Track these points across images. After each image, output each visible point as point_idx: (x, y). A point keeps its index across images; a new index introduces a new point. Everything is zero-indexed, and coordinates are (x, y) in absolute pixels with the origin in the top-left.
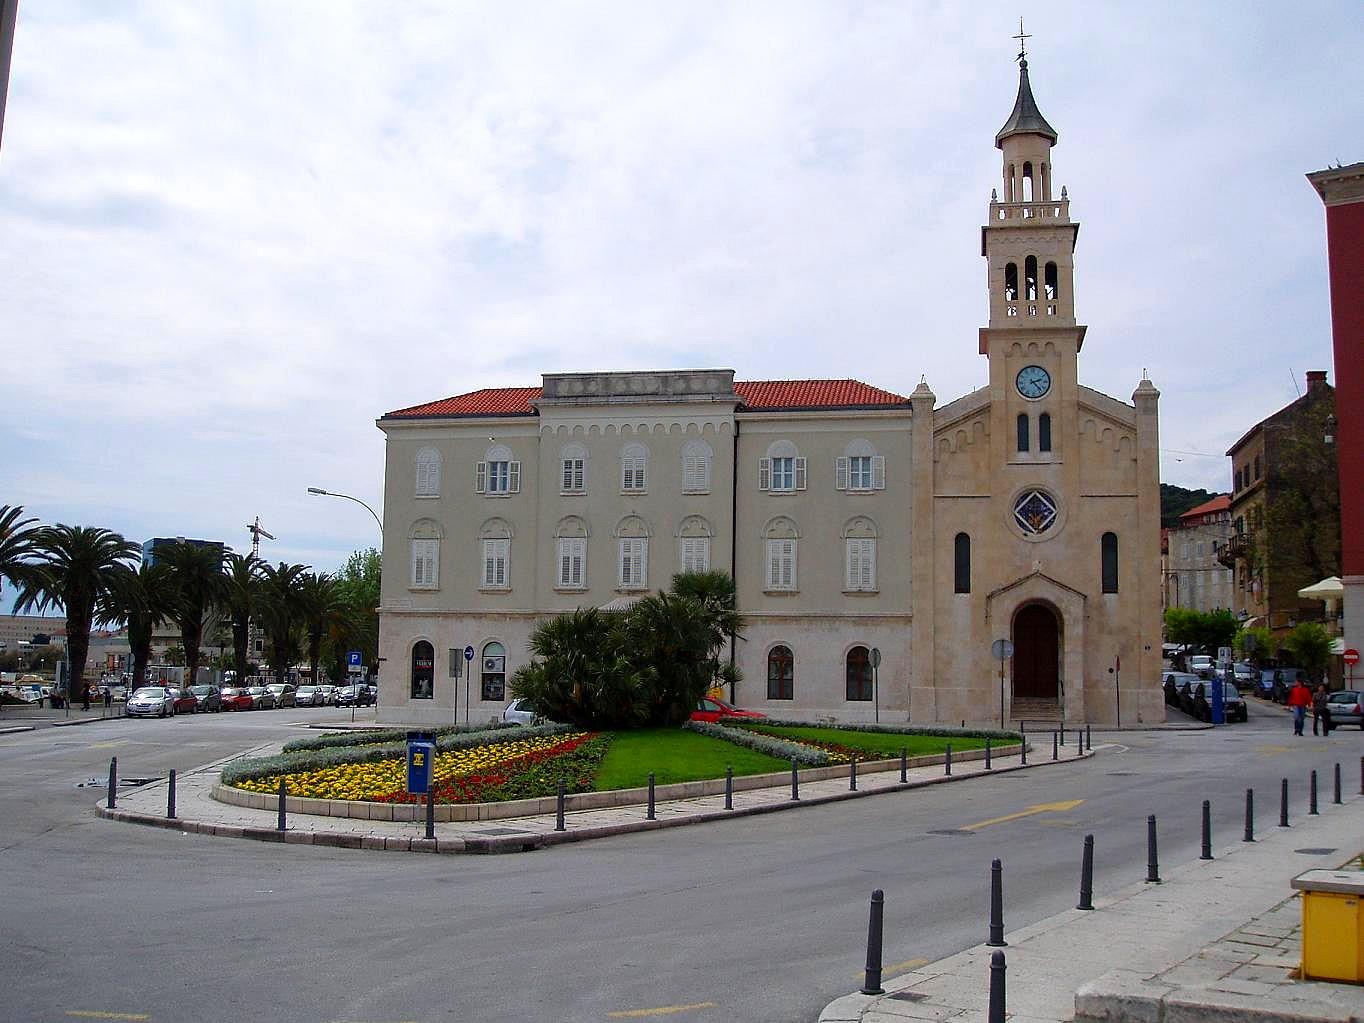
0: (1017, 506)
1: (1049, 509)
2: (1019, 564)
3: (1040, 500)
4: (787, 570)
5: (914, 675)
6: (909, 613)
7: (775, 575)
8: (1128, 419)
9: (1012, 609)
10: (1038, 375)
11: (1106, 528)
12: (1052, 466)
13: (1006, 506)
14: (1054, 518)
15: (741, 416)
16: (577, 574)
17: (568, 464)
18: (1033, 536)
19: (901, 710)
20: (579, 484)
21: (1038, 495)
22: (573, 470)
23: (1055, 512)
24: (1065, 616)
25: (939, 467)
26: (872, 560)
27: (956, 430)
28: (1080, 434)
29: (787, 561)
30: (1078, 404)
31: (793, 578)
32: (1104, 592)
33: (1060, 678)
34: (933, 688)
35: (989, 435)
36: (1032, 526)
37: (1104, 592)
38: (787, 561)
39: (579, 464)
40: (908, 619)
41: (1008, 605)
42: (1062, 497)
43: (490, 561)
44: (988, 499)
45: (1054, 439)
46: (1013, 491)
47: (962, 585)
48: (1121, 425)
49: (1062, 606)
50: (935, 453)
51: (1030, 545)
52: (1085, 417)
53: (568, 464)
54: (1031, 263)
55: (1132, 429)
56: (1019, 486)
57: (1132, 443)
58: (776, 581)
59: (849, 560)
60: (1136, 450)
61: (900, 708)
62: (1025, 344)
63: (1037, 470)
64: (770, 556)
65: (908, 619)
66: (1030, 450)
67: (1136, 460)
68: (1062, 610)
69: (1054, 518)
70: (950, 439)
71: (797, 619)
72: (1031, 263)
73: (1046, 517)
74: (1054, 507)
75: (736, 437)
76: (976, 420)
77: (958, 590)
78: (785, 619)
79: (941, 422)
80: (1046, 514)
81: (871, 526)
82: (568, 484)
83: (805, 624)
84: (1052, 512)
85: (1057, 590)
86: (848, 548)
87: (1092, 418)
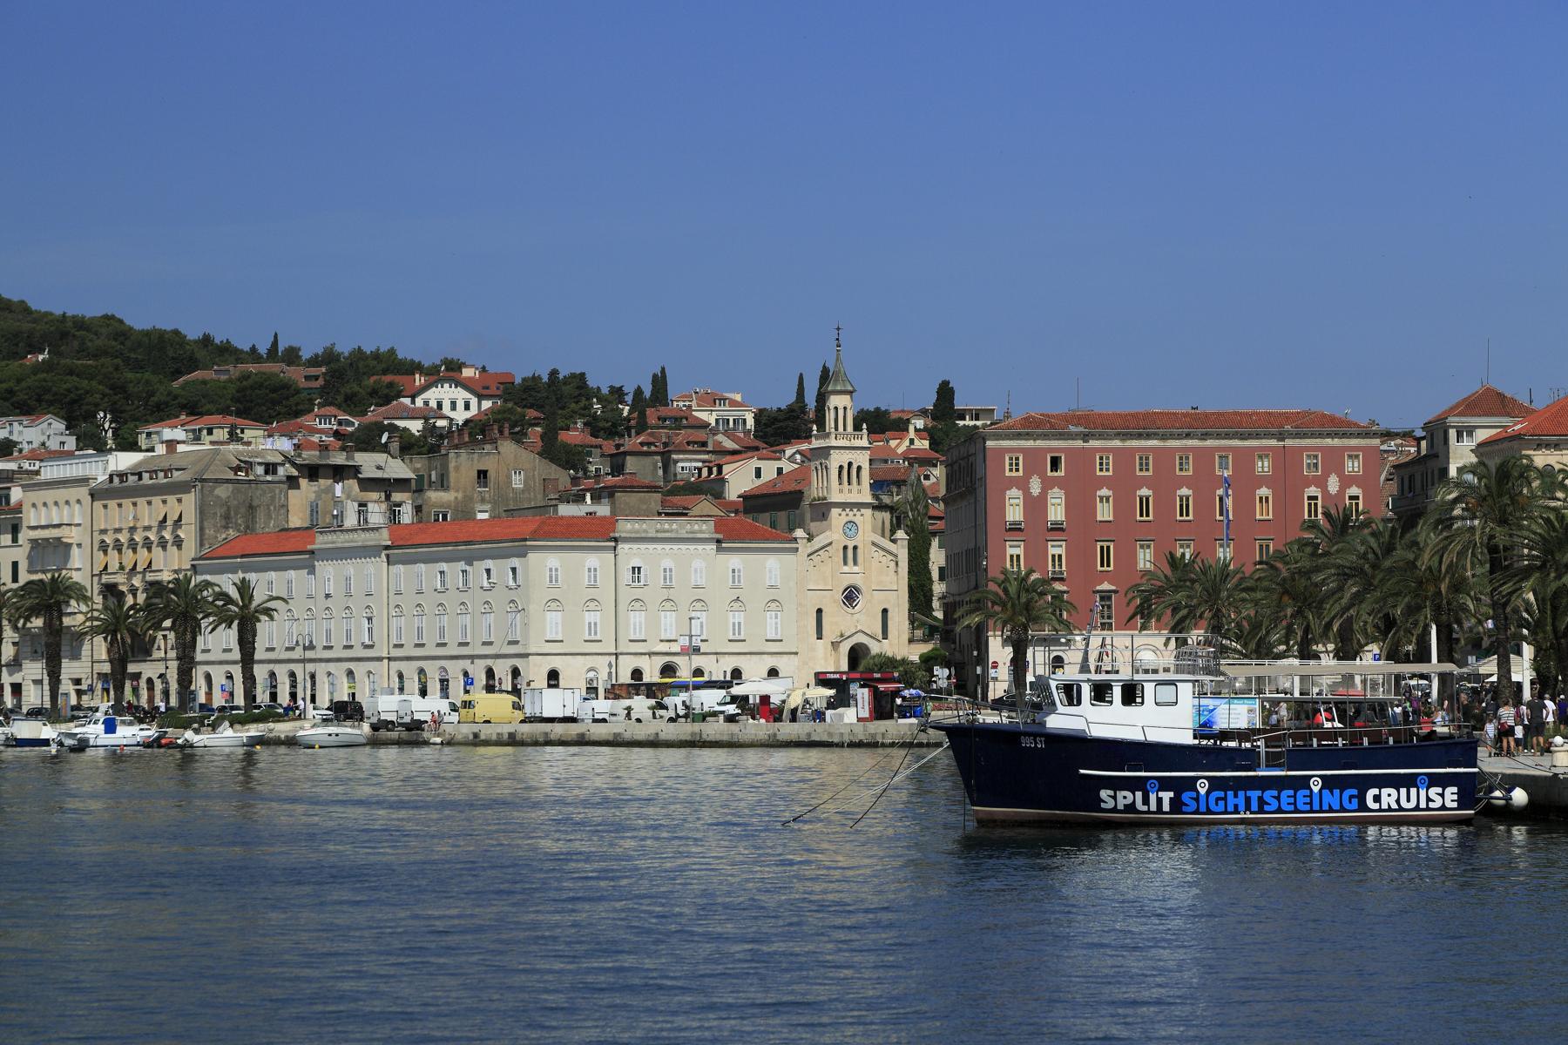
13: (839, 596)
16: (640, 631)
18: (850, 610)
47: (820, 638)
63: (853, 575)
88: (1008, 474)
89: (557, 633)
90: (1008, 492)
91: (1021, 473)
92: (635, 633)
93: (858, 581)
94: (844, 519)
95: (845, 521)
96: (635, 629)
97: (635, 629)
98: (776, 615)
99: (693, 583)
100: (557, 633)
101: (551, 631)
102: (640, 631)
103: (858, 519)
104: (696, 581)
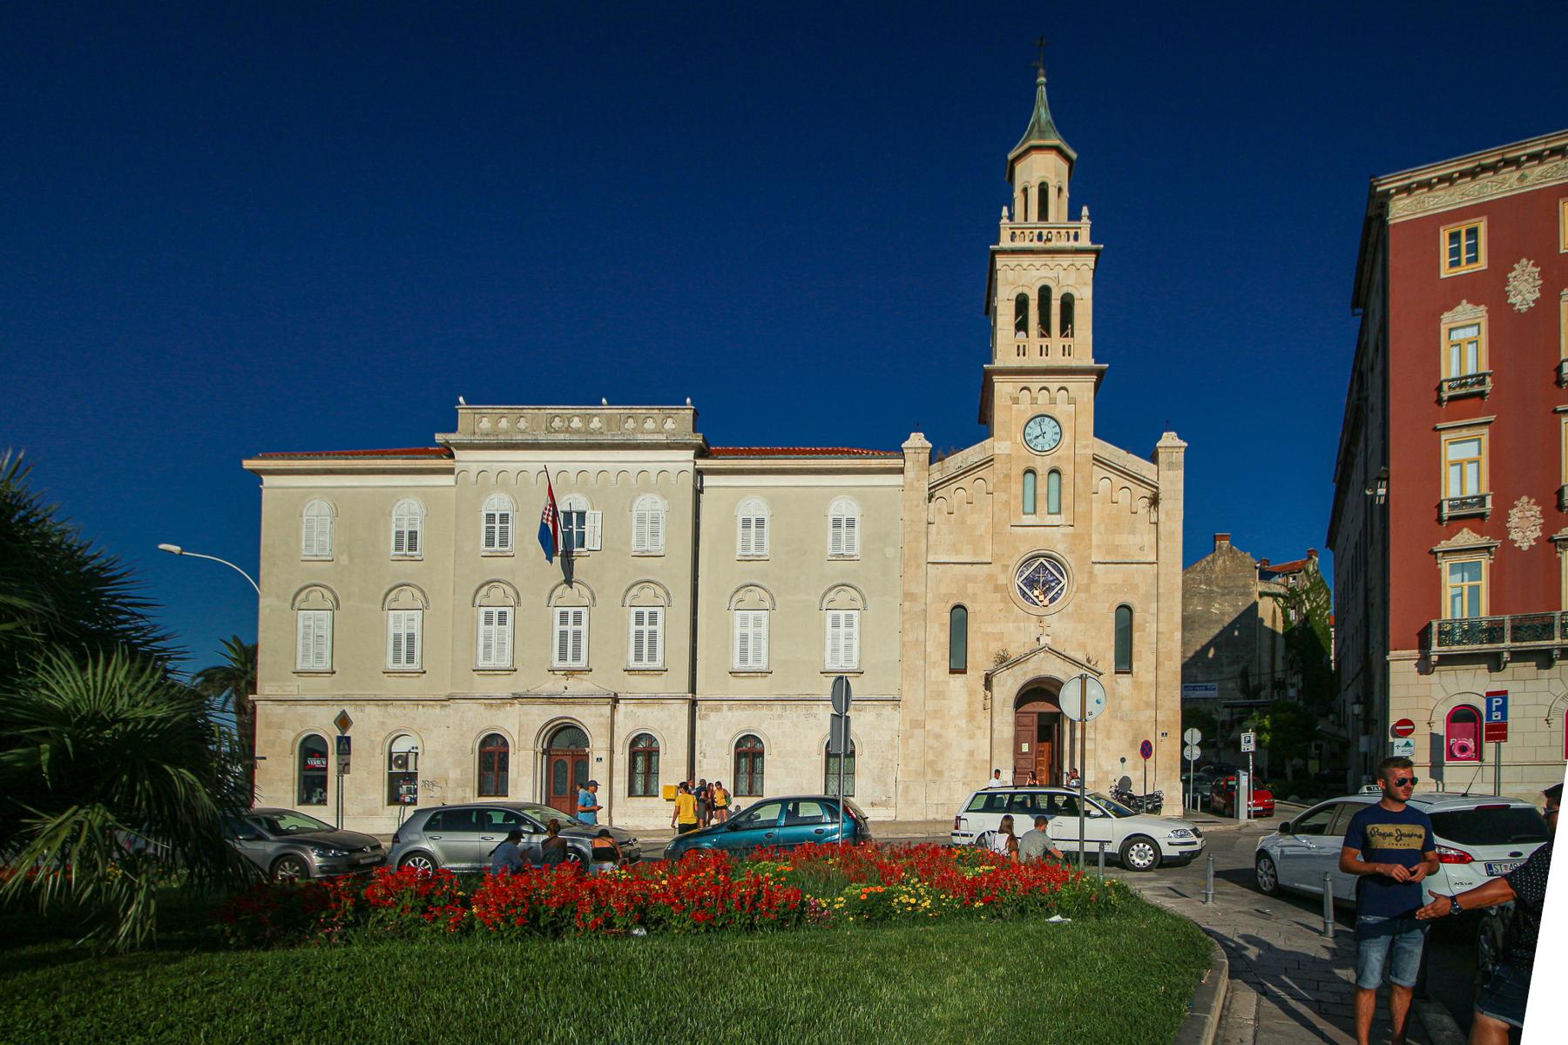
4: (757, 649)
7: (744, 651)
11: (1121, 600)
15: (703, 463)
16: (501, 651)
17: (490, 517)
20: (504, 543)
21: (1044, 562)
22: (497, 525)
23: (1064, 581)
26: (856, 635)
29: (757, 636)
36: (1037, 597)
37: (1116, 673)
38: (757, 636)
39: (504, 518)
40: (896, 701)
41: (1009, 685)
42: (1072, 565)
43: (397, 638)
44: (990, 565)
53: (491, 518)
54: (1045, 293)
56: (1025, 551)
58: (744, 659)
64: (738, 631)
65: (896, 701)
69: (1062, 589)
72: (1045, 293)
73: (1053, 588)
75: (698, 492)
77: (952, 671)
78: (755, 702)
82: (490, 542)
83: (778, 709)
88: (1445, 272)
89: (319, 656)
90: (1447, 317)
91: (1482, 264)
92: (487, 657)
93: (1056, 541)
94: (1025, 409)
95: (1030, 415)
96: (487, 646)
97: (487, 646)
98: (849, 617)
99: (634, 547)
100: (319, 656)
101: (305, 656)
102: (501, 651)
103: (1062, 410)
104: (641, 541)
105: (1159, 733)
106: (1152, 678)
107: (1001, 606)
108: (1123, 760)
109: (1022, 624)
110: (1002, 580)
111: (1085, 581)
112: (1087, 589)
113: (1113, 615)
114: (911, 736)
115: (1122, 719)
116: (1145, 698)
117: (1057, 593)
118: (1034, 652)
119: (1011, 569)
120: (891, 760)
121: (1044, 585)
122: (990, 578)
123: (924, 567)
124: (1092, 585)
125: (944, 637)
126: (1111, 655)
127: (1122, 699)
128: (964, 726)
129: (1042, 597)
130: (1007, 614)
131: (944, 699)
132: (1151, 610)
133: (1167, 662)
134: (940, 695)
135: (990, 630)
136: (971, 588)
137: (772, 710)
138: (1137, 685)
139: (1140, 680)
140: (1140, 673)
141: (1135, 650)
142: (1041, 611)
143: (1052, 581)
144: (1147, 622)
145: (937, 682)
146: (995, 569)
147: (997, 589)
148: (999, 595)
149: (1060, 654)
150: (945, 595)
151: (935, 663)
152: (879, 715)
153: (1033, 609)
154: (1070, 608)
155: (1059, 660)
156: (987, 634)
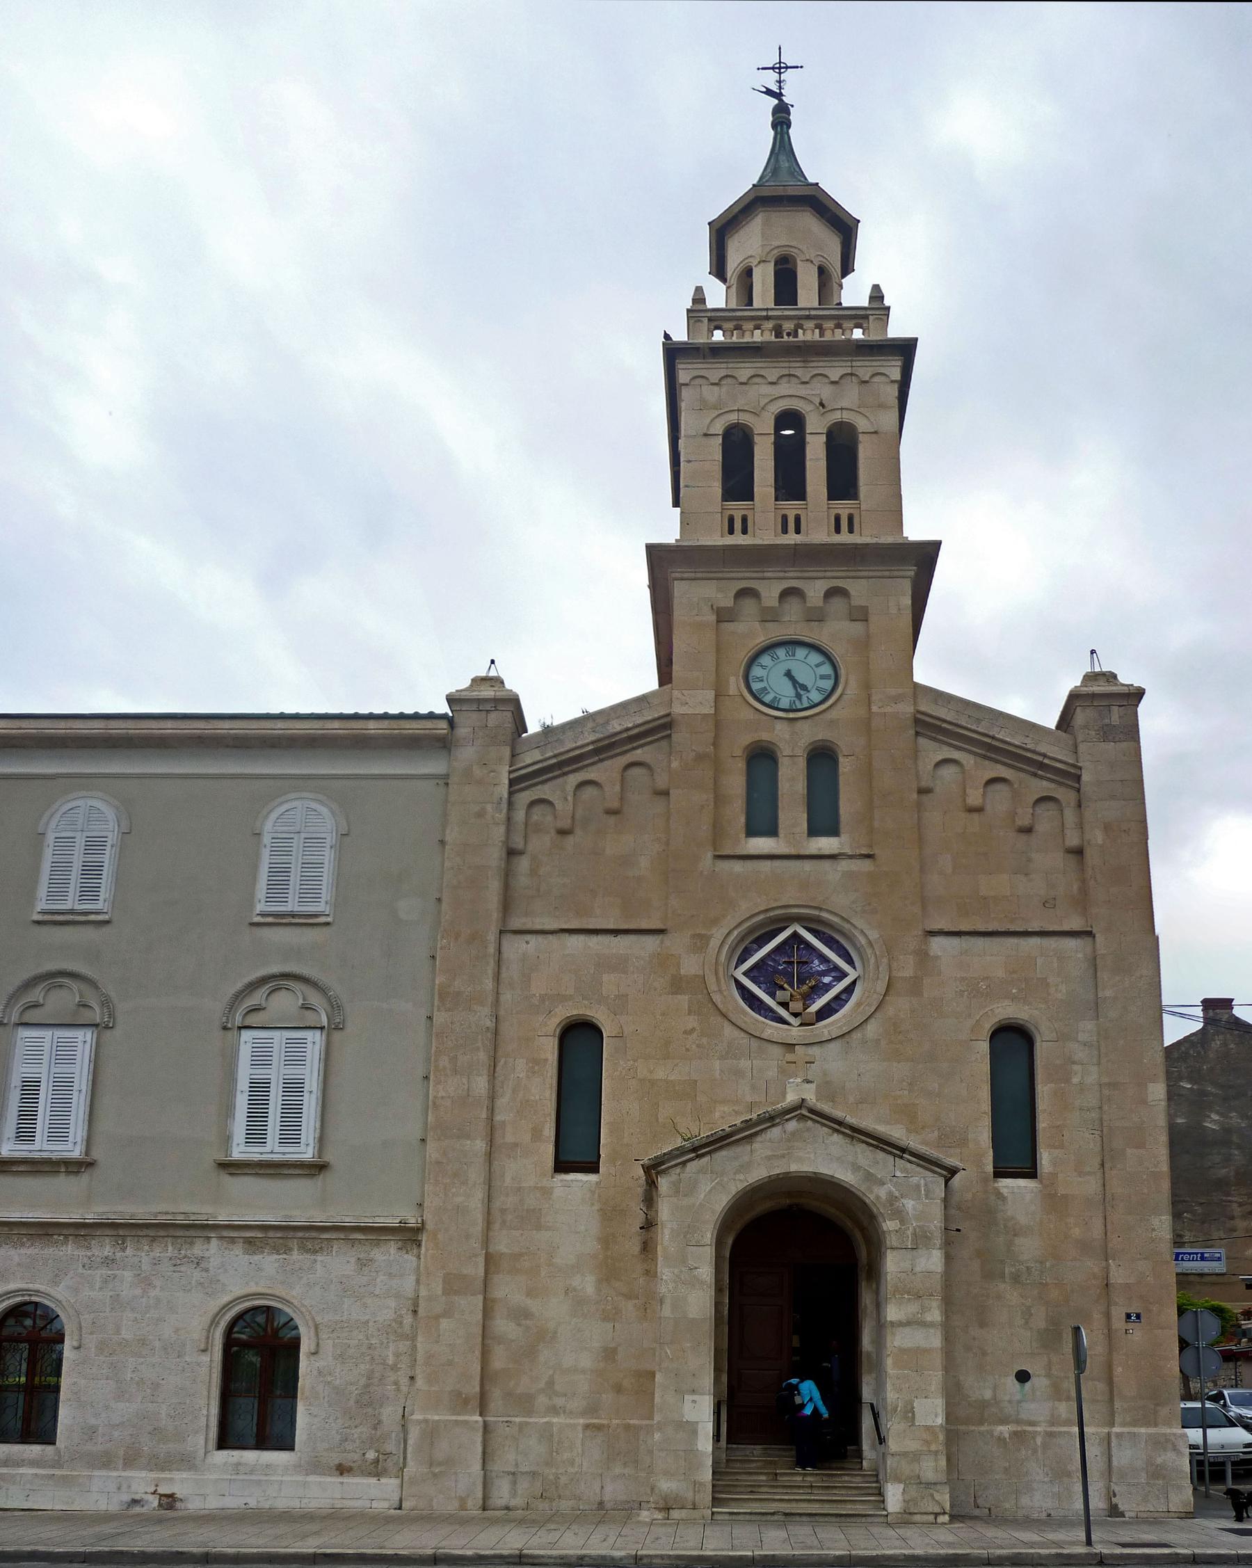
0: (742, 960)
1: (836, 968)
2: (749, 1099)
3: (809, 946)
5: (420, 1383)
6: (412, 1222)
8: (1058, 752)
9: (721, 1202)
10: (807, 667)
12: (844, 865)
14: (849, 990)
19: (378, 1475)
24: (889, 1225)
25: (523, 864)
27: (573, 779)
28: (923, 791)
30: (917, 721)
31: (77, 1130)
32: (998, 1174)
33: (867, 1394)
34: (480, 1419)
35: (665, 793)
36: (785, 1005)
40: (409, 1236)
42: (873, 935)
45: (848, 805)
46: (730, 921)
48: (1037, 765)
49: (876, 1195)
50: (508, 831)
51: (776, 1051)
52: (933, 752)
55: (1071, 777)
57: (1070, 815)
59: (243, 1084)
60: (1081, 826)
61: (376, 1470)
62: (770, 592)
65: (409, 1236)
66: (781, 832)
67: (1078, 852)
68: (879, 1209)
69: (849, 990)
70: (556, 802)
71: (82, 1231)
74: (850, 962)
76: (638, 755)
79: (530, 758)
80: (827, 980)
81: (315, 999)
84: (844, 975)
85: (864, 1155)
86: (245, 1053)
87: (956, 755)
105: (1118, 1313)
106: (1091, 1186)
107: (692, 1022)
108: (1023, 1377)
109: (744, 1064)
110: (690, 966)
111: (908, 972)
112: (915, 986)
113: (985, 1047)
114: (447, 1313)
115: (1016, 1279)
116: (1076, 1232)
117: (837, 998)
118: (771, 1119)
119: (714, 943)
120: (394, 1368)
121: (801, 981)
122: (663, 961)
123: (492, 937)
124: (927, 981)
125: (544, 1091)
126: (983, 1135)
127: (1015, 1235)
128: (590, 1290)
129: (796, 1006)
130: (704, 1040)
131: (539, 1227)
132: (1082, 1037)
133: (1129, 1151)
134: (532, 1219)
135: (660, 1074)
136: (610, 984)
137: (89, 1248)
138: (1054, 1202)
139: (1061, 1191)
140: (1061, 1176)
141: (1043, 1124)
142: (795, 1032)
143: (824, 973)
144: (1074, 1063)
145: (519, 1189)
146: (676, 943)
147: (678, 985)
148: (683, 1000)
149: (840, 1123)
150: (543, 998)
151: (516, 1145)
152: (362, 1264)
153: (771, 1029)
154: (871, 1029)
155: (836, 1137)
156: (653, 1083)
